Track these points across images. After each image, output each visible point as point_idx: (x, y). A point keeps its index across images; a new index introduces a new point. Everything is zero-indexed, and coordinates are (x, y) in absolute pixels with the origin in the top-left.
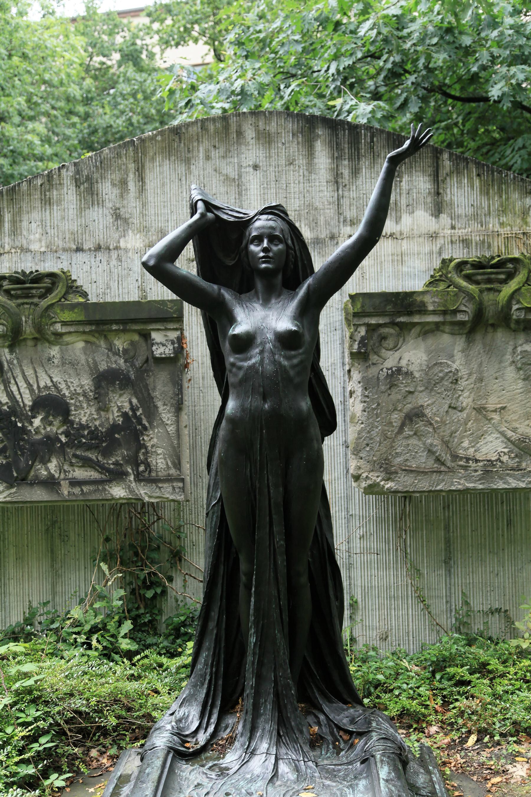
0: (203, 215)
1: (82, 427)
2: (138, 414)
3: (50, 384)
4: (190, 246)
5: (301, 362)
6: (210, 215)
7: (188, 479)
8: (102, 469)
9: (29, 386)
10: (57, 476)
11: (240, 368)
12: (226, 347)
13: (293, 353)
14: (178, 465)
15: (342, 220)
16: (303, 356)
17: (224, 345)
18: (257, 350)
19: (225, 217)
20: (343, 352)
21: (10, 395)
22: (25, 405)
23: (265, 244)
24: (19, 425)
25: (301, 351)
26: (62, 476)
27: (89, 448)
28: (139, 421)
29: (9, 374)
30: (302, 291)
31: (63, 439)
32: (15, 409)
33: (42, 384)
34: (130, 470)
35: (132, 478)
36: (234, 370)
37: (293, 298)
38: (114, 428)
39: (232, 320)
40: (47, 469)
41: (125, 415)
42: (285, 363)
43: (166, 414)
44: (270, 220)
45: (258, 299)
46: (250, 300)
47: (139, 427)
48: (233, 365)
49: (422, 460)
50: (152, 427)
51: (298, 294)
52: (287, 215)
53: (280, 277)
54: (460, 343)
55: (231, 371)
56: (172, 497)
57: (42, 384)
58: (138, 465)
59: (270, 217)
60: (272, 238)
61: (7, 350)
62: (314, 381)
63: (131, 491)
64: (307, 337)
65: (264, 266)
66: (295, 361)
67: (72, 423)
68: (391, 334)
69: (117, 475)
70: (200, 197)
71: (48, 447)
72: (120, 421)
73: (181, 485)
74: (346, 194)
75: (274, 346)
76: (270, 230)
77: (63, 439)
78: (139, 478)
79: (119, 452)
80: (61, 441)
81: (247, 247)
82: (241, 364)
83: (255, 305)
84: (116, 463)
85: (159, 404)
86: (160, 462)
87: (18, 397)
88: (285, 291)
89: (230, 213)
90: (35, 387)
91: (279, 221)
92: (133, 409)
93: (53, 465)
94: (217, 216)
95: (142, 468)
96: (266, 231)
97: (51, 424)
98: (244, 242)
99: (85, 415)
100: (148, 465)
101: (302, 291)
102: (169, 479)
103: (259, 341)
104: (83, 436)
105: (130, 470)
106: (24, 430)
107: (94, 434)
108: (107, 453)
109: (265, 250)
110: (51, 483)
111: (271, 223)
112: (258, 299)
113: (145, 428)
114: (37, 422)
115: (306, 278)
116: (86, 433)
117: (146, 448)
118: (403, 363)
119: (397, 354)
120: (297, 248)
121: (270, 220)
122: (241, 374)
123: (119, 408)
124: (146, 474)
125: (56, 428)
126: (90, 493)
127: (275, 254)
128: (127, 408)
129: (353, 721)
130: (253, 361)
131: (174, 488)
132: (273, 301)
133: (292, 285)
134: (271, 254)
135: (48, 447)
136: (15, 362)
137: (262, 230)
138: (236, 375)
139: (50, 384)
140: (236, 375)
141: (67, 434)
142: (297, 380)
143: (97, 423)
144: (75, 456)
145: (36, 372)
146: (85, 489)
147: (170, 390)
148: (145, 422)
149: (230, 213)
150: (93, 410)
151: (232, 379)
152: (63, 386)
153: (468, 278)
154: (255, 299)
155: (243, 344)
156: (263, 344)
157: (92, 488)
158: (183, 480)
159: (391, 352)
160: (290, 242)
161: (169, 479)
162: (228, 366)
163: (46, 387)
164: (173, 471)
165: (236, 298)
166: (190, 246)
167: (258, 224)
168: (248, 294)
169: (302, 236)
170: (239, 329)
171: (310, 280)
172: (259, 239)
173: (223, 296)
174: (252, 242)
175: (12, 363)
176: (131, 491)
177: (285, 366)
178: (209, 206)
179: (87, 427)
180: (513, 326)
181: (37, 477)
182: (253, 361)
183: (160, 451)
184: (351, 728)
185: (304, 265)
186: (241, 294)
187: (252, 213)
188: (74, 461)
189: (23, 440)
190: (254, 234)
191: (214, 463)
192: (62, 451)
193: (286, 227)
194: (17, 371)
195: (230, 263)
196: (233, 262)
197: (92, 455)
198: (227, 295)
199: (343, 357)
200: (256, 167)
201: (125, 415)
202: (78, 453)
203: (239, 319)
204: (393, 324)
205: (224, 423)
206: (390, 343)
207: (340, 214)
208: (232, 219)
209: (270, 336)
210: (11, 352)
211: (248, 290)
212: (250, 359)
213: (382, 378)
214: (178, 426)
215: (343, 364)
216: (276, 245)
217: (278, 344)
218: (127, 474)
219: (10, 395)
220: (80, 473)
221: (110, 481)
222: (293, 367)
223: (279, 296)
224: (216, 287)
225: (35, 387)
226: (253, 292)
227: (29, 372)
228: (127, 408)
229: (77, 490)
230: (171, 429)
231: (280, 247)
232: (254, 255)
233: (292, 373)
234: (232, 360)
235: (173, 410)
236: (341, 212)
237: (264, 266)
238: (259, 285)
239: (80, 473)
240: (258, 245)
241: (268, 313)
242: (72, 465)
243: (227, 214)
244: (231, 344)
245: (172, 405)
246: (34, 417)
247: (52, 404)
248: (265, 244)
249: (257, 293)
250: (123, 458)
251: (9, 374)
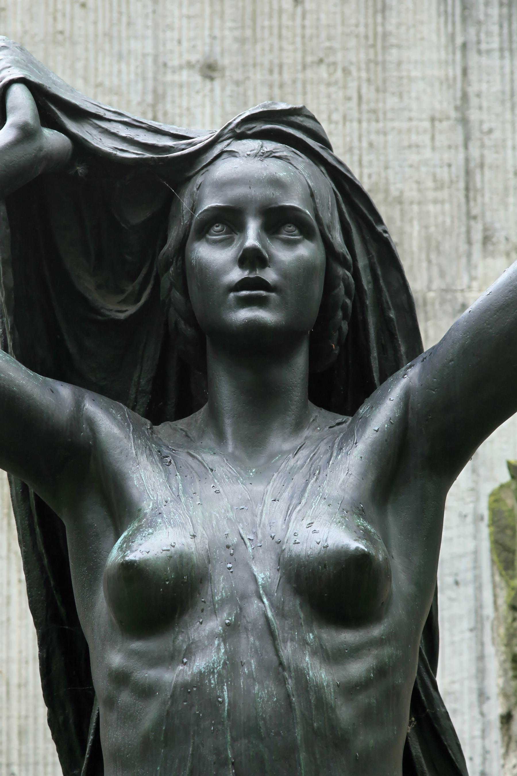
0: (26, 134)
5: (381, 672)
6: (52, 139)
11: (146, 692)
12: (97, 612)
13: (348, 637)
15: (477, 236)
16: (387, 651)
17: (90, 607)
18: (214, 625)
19: (106, 145)
20: (481, 658)
23: (252, 235)
25: (377, 631)
30: (383, 413)
36: (125, 697)
37: (349, 436)
39: (120, 510)
42: (321, 674)
44: (270, 155)
45: (221, 436)
46: (189, 441)
48: (121, 678)
51: (365, 422)
52: (327, 145)
53: (300, 362)
55: (111, 703)
59: (269, 146)
60: (277, 220)
62: (417, 750)
64: (400, 582)
65: (244, 315)
66: (357, 669)
70: (17, 74)
74: (490, 157)
75: (280, 612)
76: (270, 192)
81: (182, 249)
82: (151, 674)
83: (208, 458)
88: (318, 414)
89: (124, 132)
91: (302, 162)
96: (257, 193)
98: (174, 235)
101: (383, 413)
103: (220, 586)
109: (252, 259)
111: (274, 168)
112: (221, 436)
115: (391, 368)
120: (362, 263)
121: (270, 155)
122: (151, 713)
127: (284, 274)
130: (199, 664)
132: (279, 442)
133: (341, 391)
134: (270, 275)
137: (240, 191)
138: (129, 717)
140: (129, 717)
142: (366, 740)
149: (124, 132)
154: (209, 441)
155: (161, 601)
156: (237, 600)
160: (337, 238)
162: (100, 682)
165: (138, 432)
167: (224, 169)
168: (181, 424)
169: (379, 220)
170: (150, 545)
171: (409, 378)
172: (229, 219)
173: (91, 423)
174: (203, 230)
177: (319, 689)
178: (50, 106)
182: (199, 664)
185: (385, 324)
186: (156, 420)
187: (202, 136)
190: (210, 202)
193: (325, 186)
195: (120, 310)
196: (132, 310)
198: (108, 424)
199: (481, 673)
200: (210, 70)
203: (147, 507)
207: (470, 217)
208: (132, 153)
209: (265, 573)
211: (184, 410)
212: (189, 653)
215: (482, 696)
216: (291, 244)
217: (293, 603)
222: (350, 690)
223: (298, 426)
224: (65, 391)
226: (200, 415)
231: (306, 250)
232: (206, 276)
233: (345, 713)
234: (116, 659)
236: (475, 211)
237: (244, 315)
238: (225, 389)
240: (226, 243)
241: (258, 488)
243: (115, 135)
244: (117, 603)
248: (252, 235)
249: (215, 418)
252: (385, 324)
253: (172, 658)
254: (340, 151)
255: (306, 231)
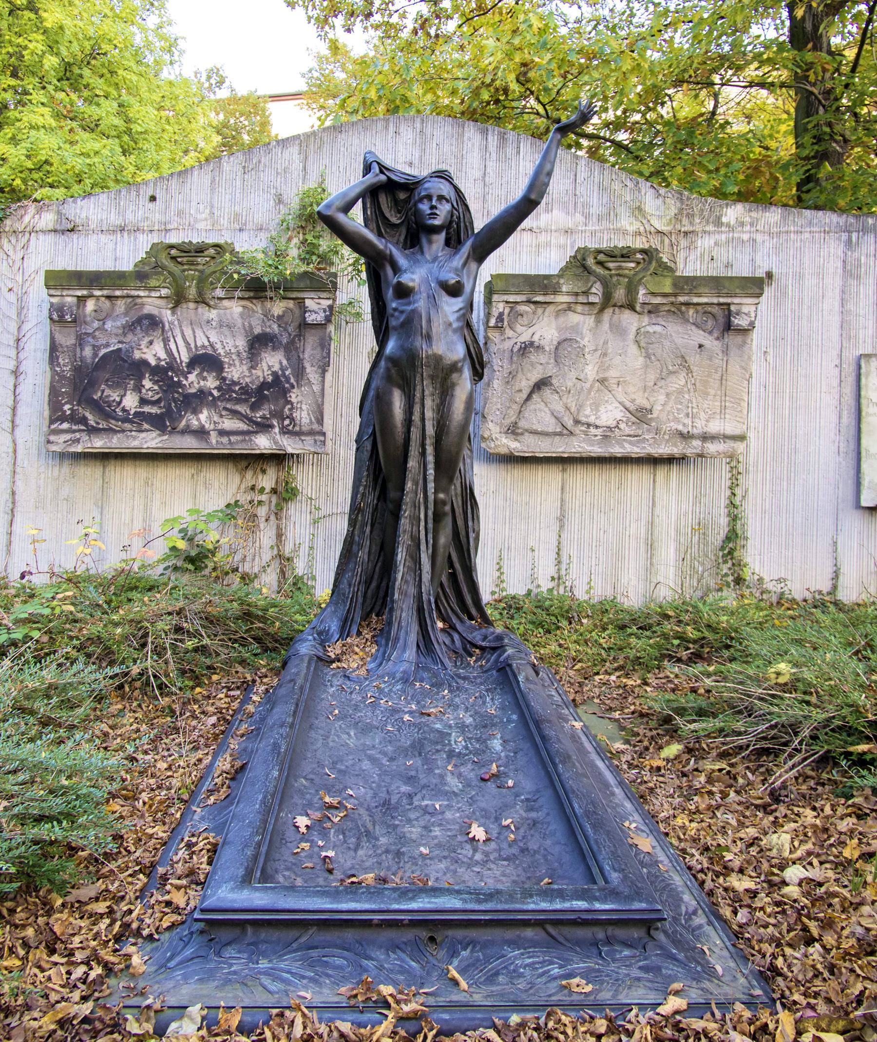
1: (234, 383)
2: (287, 373)
3: (207, 343)
4: (360, 200)
7: (329, 435)
8: (251, 420)
9: (187, 344)
10: (207, 426)
11: (402, 312)
14: (320, 421)
21: (169, 353)
22: (181, 362)
24: (176, 379)
25: (460, 299)
26: (212, 427)
27: (238, 401)
28: (288, 380)
29: (170, 334)
31: (216, 393)
32: (172, 365)
33: (199, 344)
34: (275, 423)
35: (277, 430)
36: (396, 314)
38: (264, 385)
40: (198, 419)
41: (275, 374)
43: (311, 372)
47: (287, 385)
48: (395, 310)
49: (551, 425)
50: (299, 386)
54: (590, 321)
55: (392, 316)
56: (313, 450)
57: (199, 344)
58: (283, 419)
61: (169, 312)
63: (276, 443)
67: (224, 379)
68: (527, 312)
69: (264, 427)
71: (201, 398)
72: (270, 379)
73: (322, 438)
77: (216, 393)
78: (284, 431)
79: (266, 406)
80: (212, 395)
81: (415, 205)
84: (263, 417)
85: (307, 365)
86: (304, 416)
87: (176, 355)
90: (193, 346)
92: (283, 369)
93: (204, 416)
94: (388, 178)
95: (287, 422)
97: (205, 379)
99: (237, 372)
100: (292, 420)
102: (311, 433)
104: (234, 392)
105: (275, 423)
106: (179, 384)
107: (245, 390)
108: (254, 407)
110: (201, 433)
113: (293, 387)
114: (192, 377)
116: (237, 388)
117: (292, 404)
118: (536, 338)
119: (531, 331)
123: (270, 367)
124: (290, 428)
125: (211, 383)
126: (237, 442)
128: (277, 368)
129: (485, 638)
131: (315, 441)
135: (201, 398)
136: (176, 323)
138: (397, 318)
139: (207, 343)
140: (397, 318)
141: (219, 388)
143: (248, 380)
144: (225, 409)
145: (194, 332)
146: (233, 438)
147: (318, 353)
148: (292, 380)
150: (245, 368)
151: (393, 323)
152: (218, 346)
153: (600, 263)
157: (239, 438)
158: (324, 434)
159: (524, 328)
161: (311, 433)
162: (389, 311)
163: (203, 346)
164: (316, 427)
166: (360, 200)
175: (173, 324)
176: (276, 443)
179: (238, 383)
180: (638, 308)
181: (188, 426)
183: (304, 407)
184: (484, 644)
185: (466, 226)
188: (224, 413)
189: (178, 392)
191: (367, 404)
192: (213, 404)
194: (177, 332)
197: (243, 409)
201: (275, 374)
202: (229, 406)
204: (529, 301)
205: (383, 364)
206: (525, 320)
208: (403, 181)
210: (173, 313)
213: (515, 350)
214: (323, 386)
218: (272, 426)
219: (169, 353)
220: (229, 424)
221: (257, 432)
225: (193, 346)
227: (188, 333)
228: (277, 368)
229: (225, 440)
230: (316, 388)
234: (394, 305)
235: (320, 371)
239: (229, 424)
242: (221, 416)
245: (319, 367)
246: (190, 373)
247: (206, 361)
250: (270, 413)
251: (170, 334)
252: (466, 226)
253: (409, 304)
254: (456, 182)
255: (447, 201)
